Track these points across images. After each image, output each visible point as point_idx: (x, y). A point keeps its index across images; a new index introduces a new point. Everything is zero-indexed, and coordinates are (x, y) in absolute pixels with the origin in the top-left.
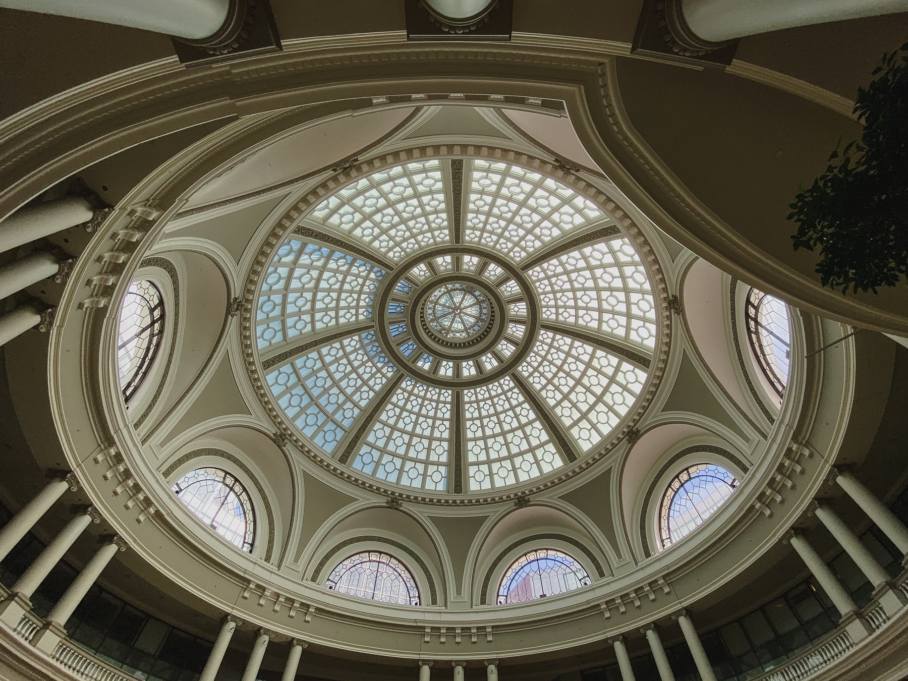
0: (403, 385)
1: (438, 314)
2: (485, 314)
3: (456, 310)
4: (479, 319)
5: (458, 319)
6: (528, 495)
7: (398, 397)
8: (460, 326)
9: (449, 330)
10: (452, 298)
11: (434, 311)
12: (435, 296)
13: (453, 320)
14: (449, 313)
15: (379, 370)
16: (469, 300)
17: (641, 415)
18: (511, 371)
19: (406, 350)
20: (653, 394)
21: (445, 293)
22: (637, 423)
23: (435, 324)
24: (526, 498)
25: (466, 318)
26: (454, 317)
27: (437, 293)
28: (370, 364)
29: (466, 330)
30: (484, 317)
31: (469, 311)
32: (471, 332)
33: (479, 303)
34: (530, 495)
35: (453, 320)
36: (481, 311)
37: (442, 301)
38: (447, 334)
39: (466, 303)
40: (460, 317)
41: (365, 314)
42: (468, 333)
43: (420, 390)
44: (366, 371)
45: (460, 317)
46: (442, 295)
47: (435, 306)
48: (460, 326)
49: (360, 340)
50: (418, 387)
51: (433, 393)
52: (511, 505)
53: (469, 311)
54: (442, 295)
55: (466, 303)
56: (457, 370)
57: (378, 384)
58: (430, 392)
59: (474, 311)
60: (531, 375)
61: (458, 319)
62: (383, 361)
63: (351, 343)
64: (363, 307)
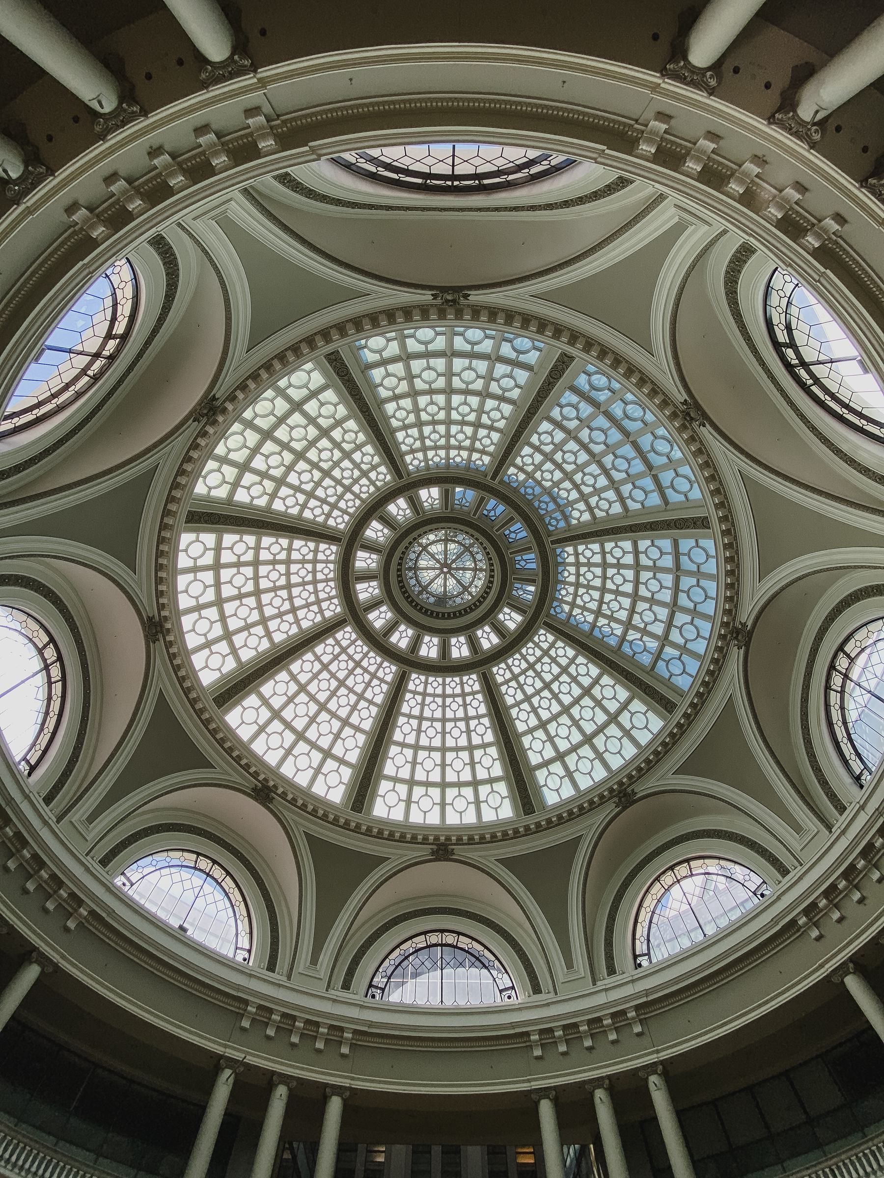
0: (487, 459)
1: (467, 556)
2: (411, 578)
3: (446, 567)
4: (416, 568)
5: (441, 557)
6: (204, 426)
7: (491, 441)
8: (433, 549)
9: (446, 541)
10: (458, 581)
11: (474, 558)
12: (480, 579)
13: (446, 555)
14: (454, 561)
15: (530, 475)
16: (437, 587)
17: (172, 657)
18: (345, 541)
19: (495, 508)
20: (181, 680)
21: (470, 586)
22: (166, 645)
23: (467, 542)
24: (205, 420)
25: (432, 563)
26: (446, 558)
27: (479, 583)
28: (548, 484)
29: (425, 548)
30: (410, 574)
31: (432, 574)
32: (416, 549)
33: (425, 588)
34: (201, 429)
35: (446, 555)
36: (417, 580)
37: (469, 575)
38: (446, 534)
39: (440, 581)
40: (438, 561)
41: (566, 555)
42: (420, 545)
43: (459, 457)
44: (549, 475)
45: (438, 561)
46: (471, 583)
47: (476, 565)
48: (433, 549)
49: (566, 518)
50: (463, 460)
51: (437, 458)
52: (220, 392)
53: (432, 574)
54: (471, 583)
55: (440, 581)
56: (414, 503)
57: (526, 456)
58: (441, 459)
59: (426, 576)
60: (316, 551)
61: (441, 557)
62: (526, 488)
63: (580, 515)
64: (570, 564)
